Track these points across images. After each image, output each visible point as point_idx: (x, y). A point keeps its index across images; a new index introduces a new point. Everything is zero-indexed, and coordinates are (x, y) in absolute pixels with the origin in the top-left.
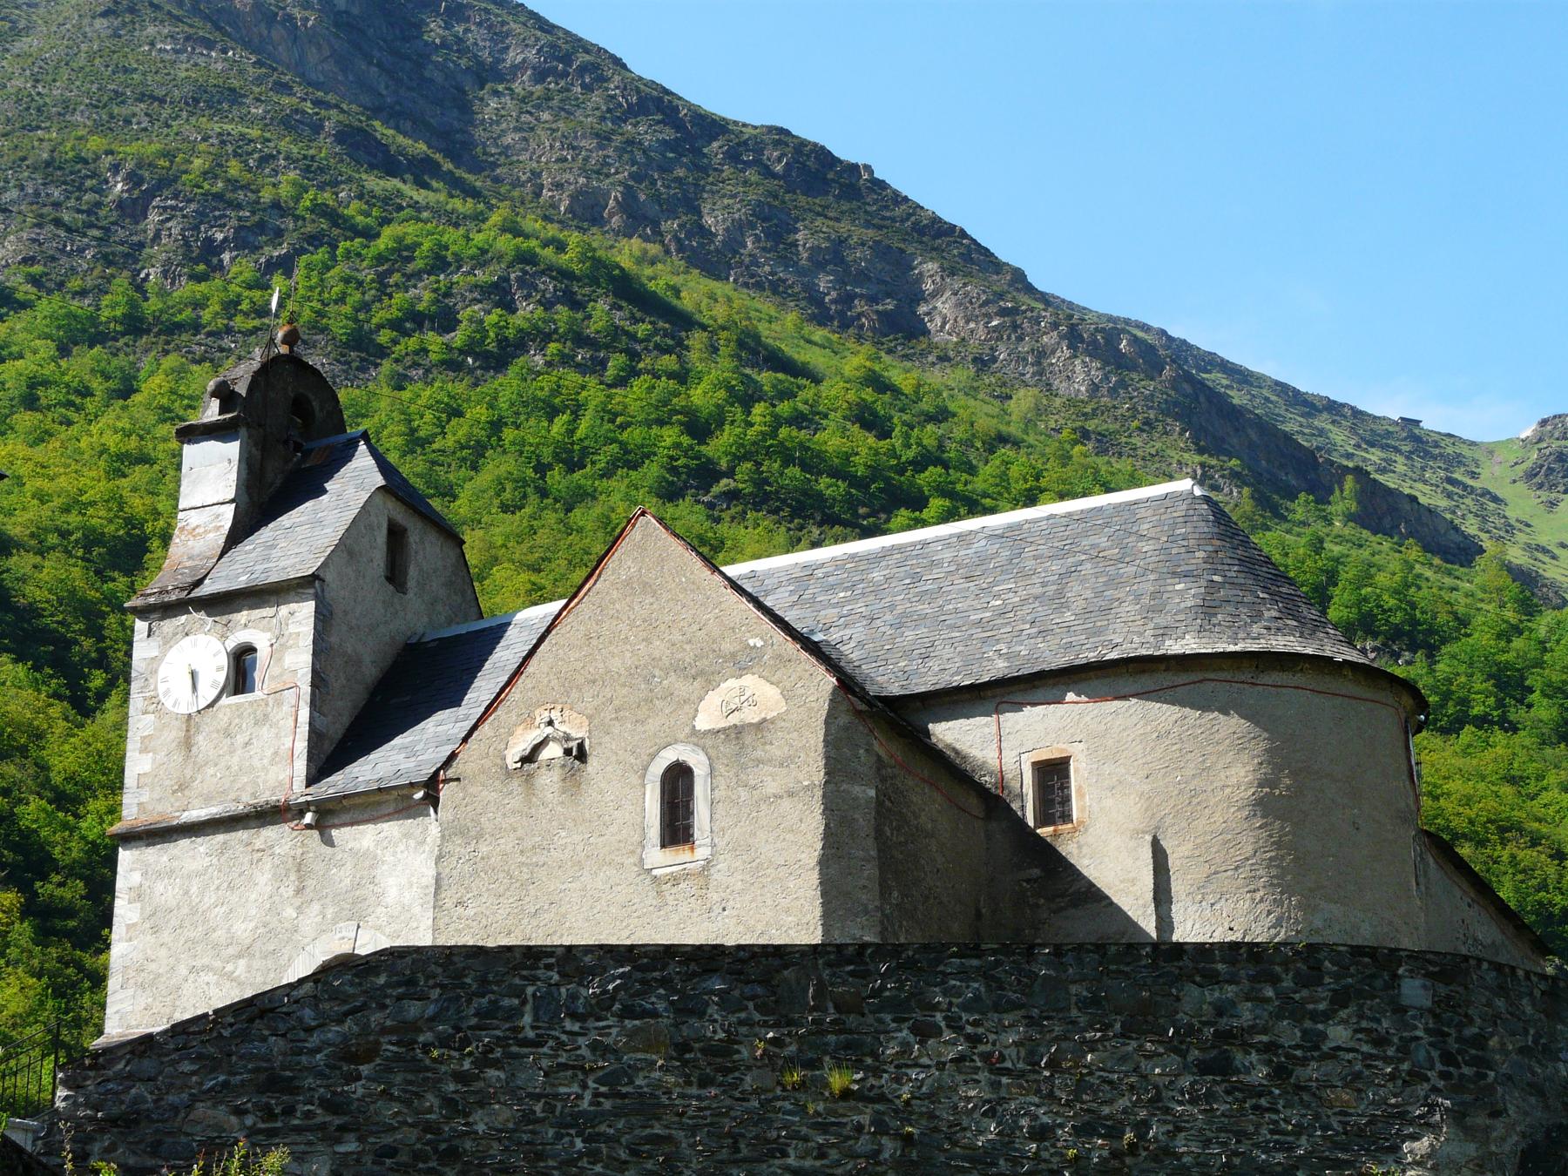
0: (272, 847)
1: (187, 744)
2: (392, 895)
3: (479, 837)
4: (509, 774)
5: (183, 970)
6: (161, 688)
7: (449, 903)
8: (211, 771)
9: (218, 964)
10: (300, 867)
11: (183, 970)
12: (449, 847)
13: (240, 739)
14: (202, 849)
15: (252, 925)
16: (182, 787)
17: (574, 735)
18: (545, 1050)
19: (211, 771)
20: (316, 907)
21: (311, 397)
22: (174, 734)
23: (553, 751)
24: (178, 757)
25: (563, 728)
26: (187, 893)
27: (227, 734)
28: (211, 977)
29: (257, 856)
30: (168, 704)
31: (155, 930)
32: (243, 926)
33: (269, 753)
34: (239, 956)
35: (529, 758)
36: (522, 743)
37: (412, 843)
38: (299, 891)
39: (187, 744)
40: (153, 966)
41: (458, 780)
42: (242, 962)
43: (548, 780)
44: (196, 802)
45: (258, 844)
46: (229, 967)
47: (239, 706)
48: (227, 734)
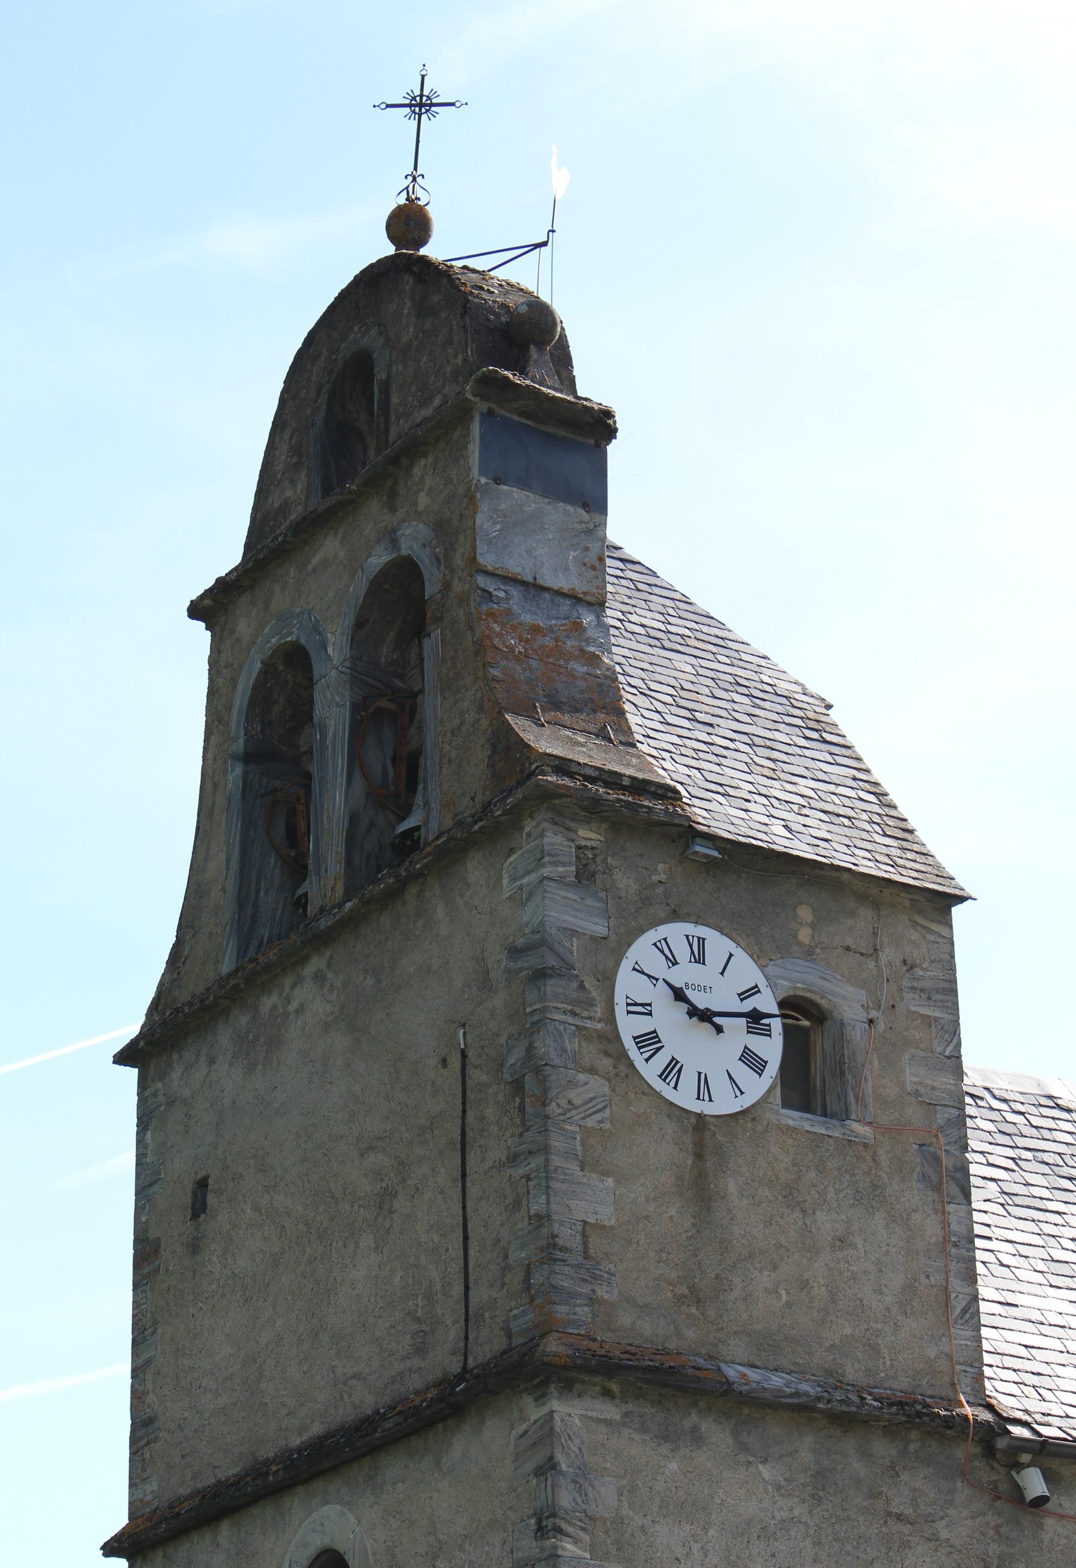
0: (930, 1520)
1: (700, 1189)
6: (629, 1027)
8: (764, 1279)
13: (826, 1224)
14: (766, 1471)
22: (662, 1152)
30: (650, 1071)
39: (700, 1189)
45: (900, 1503)
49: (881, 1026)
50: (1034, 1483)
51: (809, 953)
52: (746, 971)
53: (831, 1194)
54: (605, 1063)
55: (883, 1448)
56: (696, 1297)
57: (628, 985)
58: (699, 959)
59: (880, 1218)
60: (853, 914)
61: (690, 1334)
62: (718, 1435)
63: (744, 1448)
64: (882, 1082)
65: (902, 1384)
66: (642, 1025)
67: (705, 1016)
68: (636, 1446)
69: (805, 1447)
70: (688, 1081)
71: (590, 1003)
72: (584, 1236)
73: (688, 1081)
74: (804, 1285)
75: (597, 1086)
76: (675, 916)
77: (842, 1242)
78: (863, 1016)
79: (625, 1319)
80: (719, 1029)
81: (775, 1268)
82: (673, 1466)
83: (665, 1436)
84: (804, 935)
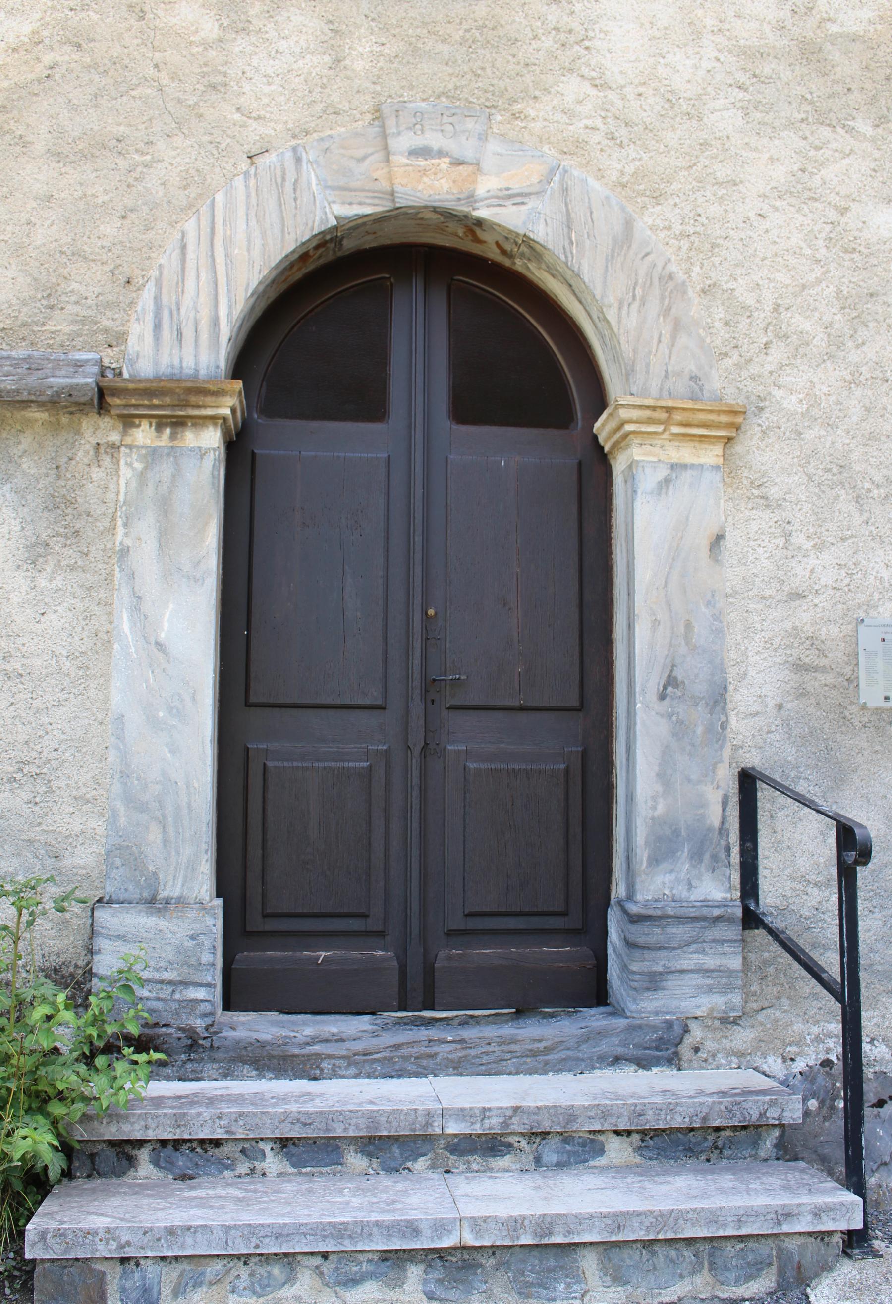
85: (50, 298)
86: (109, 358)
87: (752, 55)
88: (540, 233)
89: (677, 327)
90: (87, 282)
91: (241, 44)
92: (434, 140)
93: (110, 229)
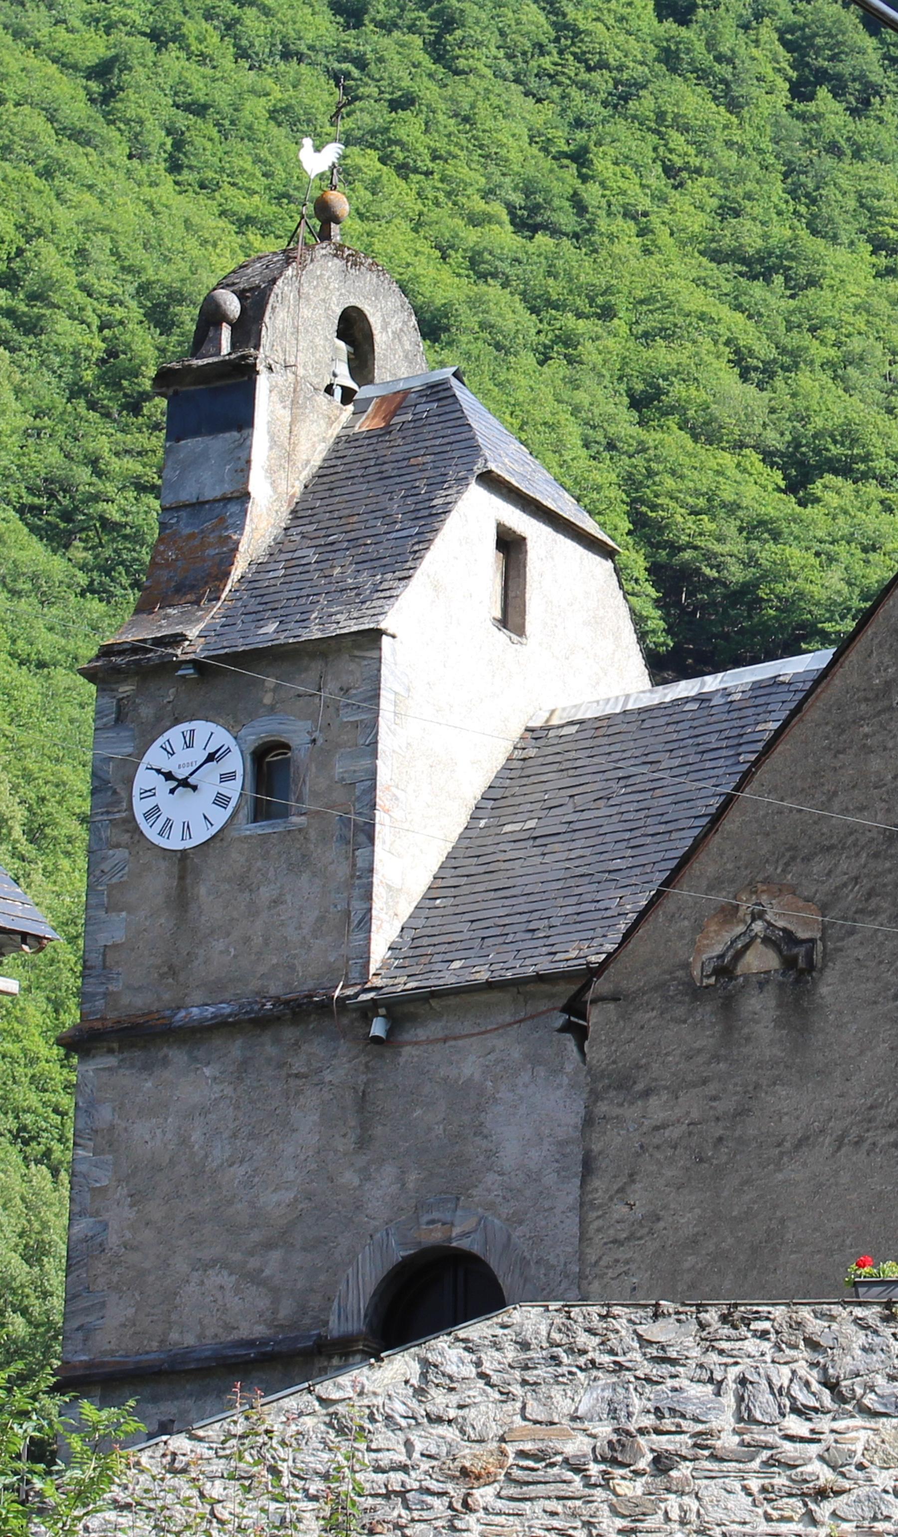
1: (181, 900)
2: (510, 1153)
3: (647, 1093)
4: (696, 993)
5: (181, 1265)
6: (140, 807)
7: (600, 1197)
8: (220, 945)
9: (236, 1257)
10: (363, 1100)
11: (181, 1265)
12: (603, 1108)
13: (266, 893)
14: (207, 1071)
15: (289, 1196)
16: (172, 971)
17: (802, 935)
18: (755, 1465)
19: (220, 945)
20: (390, 1171)
21: (368, 310)
22: (158, 883)
23: (760, 960)
24: (165, 921)
25: (780, 924)
26: (184, 1141)
27: (244, 883)
28: (228, 1280)
29: (293, 1083)
30: (151, 833)
31: (136, 1198)
32: (275, 1198)
33: (311, 916)
34: (269, 1245)
35: (724, 970)
36: (716, 945)
37: (541, 1071)
38: (363, 1142)
39: (181, 900)
40: (133, 1258)
41: (615, 999)
42: (276, 1255)
43: (760, 1007)
44: (197, 996)
45: (298, 1065)
46: (254, 1263)
47: (264, 838)
48: (244, 883)
49: (320, 741)
50: (378, 1028)
51: (272, 709)
52: (221, 737)
53: (271, 874)
54: (126, 837)
55: (289, 1034)
56: (172, 971)
57: (144, 779)
58: (189, 745)
59: (305, 877)
60: (306, 670)
61: (167, 997)
62: (178, 1056)
63: (196, 1060)
64: (312, 783)
65: (310, 985)
66: (149, 803)
67: (184, 783)
68: (126, 1079)
69: (236, 1049)
70: (177, 829)
71: (119, 802)
72: (104, 955)
73: (177, 829)
74: (247, 940)
75: (121, 854)
76: (177, 721)
77: (276, 902)
78: (308, 738)
79: (125, 1000)
80: (195, 788)
81: (228, 934)
82: (149, 1084)
83: (147, 1068)
84: (268, 699)
85: (303, 1309)
86: (323, 1331)
87: (562, 1144)
88: (476, 1249)
89: (526, 1280)
90: (315, 1301)
91: (368, 1186)
92: (435, 1215)
93: (322, 1278)
